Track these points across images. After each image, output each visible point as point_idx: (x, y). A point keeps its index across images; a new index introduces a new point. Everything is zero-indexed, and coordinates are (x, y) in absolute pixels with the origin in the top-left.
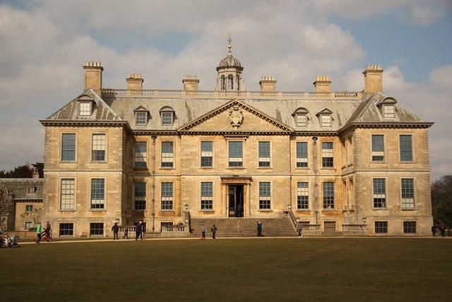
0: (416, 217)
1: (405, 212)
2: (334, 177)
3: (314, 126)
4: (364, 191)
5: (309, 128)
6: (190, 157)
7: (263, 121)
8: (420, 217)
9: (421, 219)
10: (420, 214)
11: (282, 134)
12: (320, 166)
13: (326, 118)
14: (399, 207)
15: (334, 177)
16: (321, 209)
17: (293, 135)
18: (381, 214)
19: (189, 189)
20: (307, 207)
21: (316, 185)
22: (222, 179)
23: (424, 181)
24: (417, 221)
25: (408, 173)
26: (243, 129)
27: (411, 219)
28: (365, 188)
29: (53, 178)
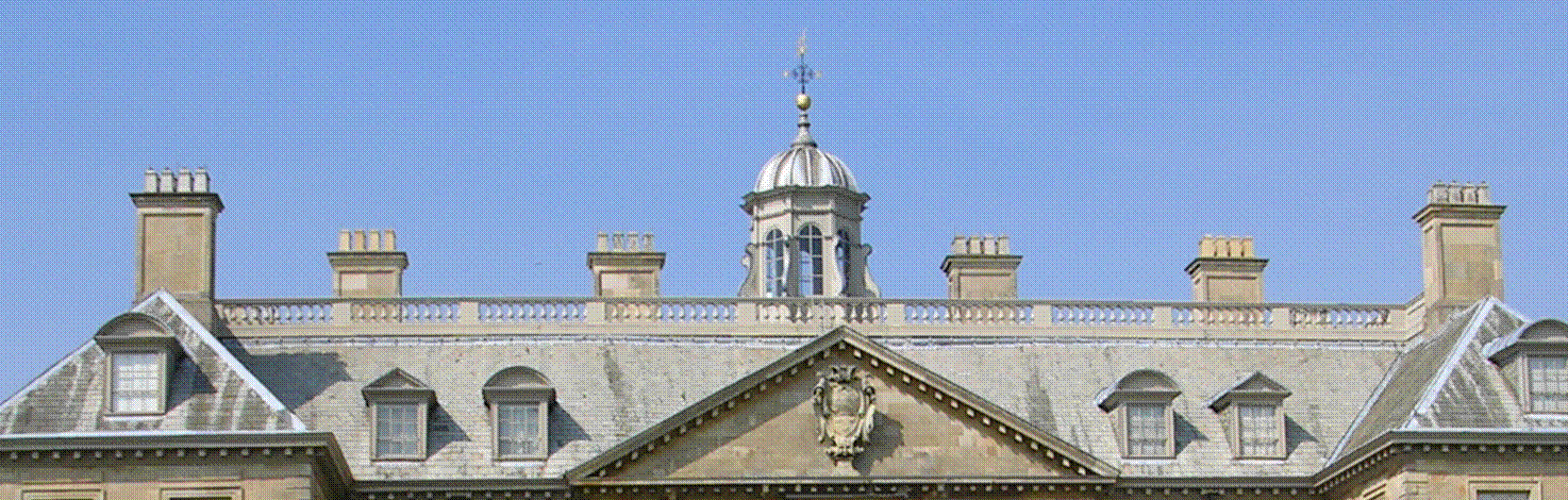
7: (970, 436)
13: (1266, 426)
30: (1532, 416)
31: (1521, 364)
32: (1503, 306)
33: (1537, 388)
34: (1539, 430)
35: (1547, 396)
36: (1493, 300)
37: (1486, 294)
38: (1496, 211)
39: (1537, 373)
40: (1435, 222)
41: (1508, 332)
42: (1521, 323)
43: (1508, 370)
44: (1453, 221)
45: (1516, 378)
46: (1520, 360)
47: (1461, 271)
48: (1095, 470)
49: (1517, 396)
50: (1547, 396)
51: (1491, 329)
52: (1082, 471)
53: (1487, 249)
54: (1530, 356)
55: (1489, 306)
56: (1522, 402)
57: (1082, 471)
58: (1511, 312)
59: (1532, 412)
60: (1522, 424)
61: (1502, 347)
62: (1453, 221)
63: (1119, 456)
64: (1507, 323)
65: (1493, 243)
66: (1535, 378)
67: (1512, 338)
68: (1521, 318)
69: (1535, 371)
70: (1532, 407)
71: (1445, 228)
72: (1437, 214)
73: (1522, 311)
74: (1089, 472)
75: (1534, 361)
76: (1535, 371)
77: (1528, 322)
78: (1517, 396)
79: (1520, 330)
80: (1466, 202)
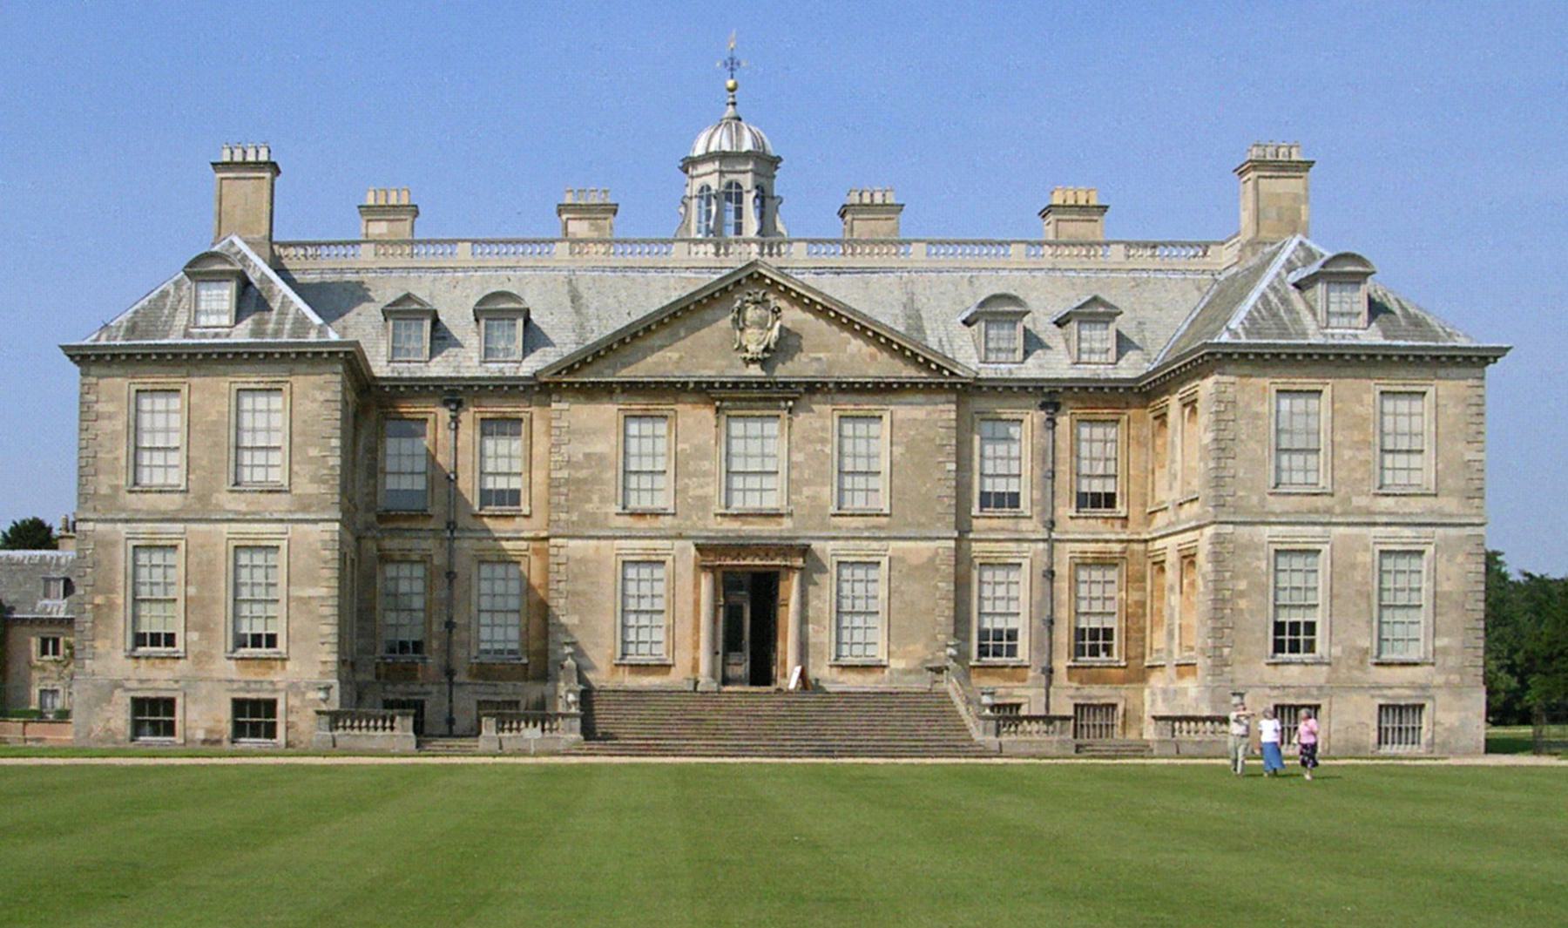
0: (1424, 688)
1: (1385, 671)
2: (1117, 547)
3: (1055, 364)
4: (1242, 594)
5: (1032, 369)
6: (583, 474)
7: (856, 345)
8: (1439, 687)
9: (1442, 697)
10: (1439, 679)
11: (928, 388)
12: (1065, 510)
13: (1101, 338)
14: (1366, 652)
15: (1117, 547)
16: (1062, 663)
17: (967, 391)
18: (1296, 675)
19: (581, 586)
20: (1012, 651)
21: (1050, 574)
22: (699, 548)
23: (1460, 559)
24: (1429, 705)
25: (1408, 532)
26: (785, 371)
27: (1405, 696)
28: (1242, 585)
29: (106, 544)
30: (1329, 331)
31: (1320, 288)
32: (1308, 243)
33: (1333, 308)
34: (1331, 341)
35: (1342, 314)
36: (1299, 237)
37: (1294, 233)
38: (1309, 164)
39: (1334, 296)
40: (1252, 175)
41: (1310, 263)
42: (1322, 256)
43: (1309, 294)
44: (1268, 174)
45: (1316, 300)
46: (1319, 285)
47: (1273, 213)
48: (956, 371)
49: (1315, 315)
50: (1342, 314)
51: (1296, 261)
52: (946, 373)
53: (1296, 197)
54: (1328, 283)
55: (1295, 241)
56: (1319, 318)
57: (946, 373)
58: (1314, 247)
59: (1327, 327)
60: (1320, 337)
61: (1305, 275)
62: (1268, 174)
63: (977, 361)
64: (1310, 256)
65: (1302, 192)
66: (1332, 299)
67: (1315, 268)
68: (1322, 250)
69: (1332, 294)
70: (1328, 323)
71: (1261, 180)
72: (1255, 168)
73: (1325, 247)
74: (952, 373)
75: (1332, 285)
76: (1332, 294)
77: (1328, 255)
78: (1315, 315)
79: (1321, 262)
80: (1280, 158)
